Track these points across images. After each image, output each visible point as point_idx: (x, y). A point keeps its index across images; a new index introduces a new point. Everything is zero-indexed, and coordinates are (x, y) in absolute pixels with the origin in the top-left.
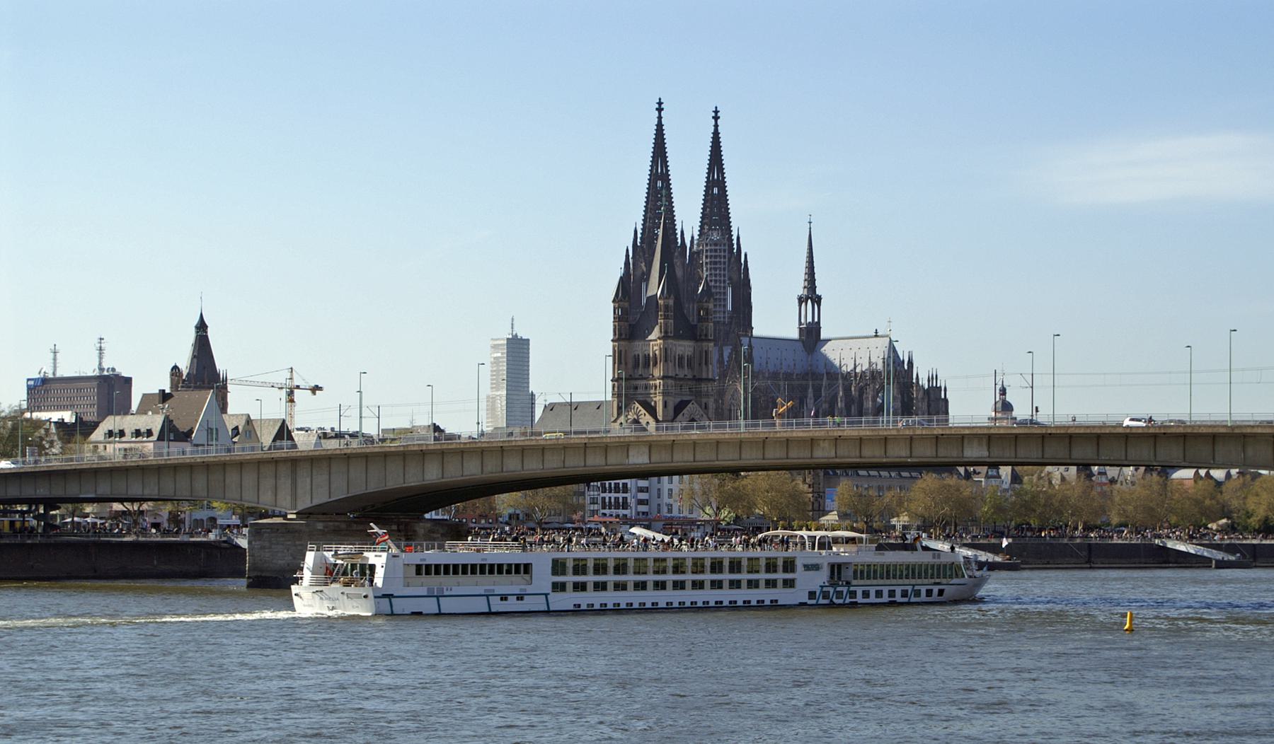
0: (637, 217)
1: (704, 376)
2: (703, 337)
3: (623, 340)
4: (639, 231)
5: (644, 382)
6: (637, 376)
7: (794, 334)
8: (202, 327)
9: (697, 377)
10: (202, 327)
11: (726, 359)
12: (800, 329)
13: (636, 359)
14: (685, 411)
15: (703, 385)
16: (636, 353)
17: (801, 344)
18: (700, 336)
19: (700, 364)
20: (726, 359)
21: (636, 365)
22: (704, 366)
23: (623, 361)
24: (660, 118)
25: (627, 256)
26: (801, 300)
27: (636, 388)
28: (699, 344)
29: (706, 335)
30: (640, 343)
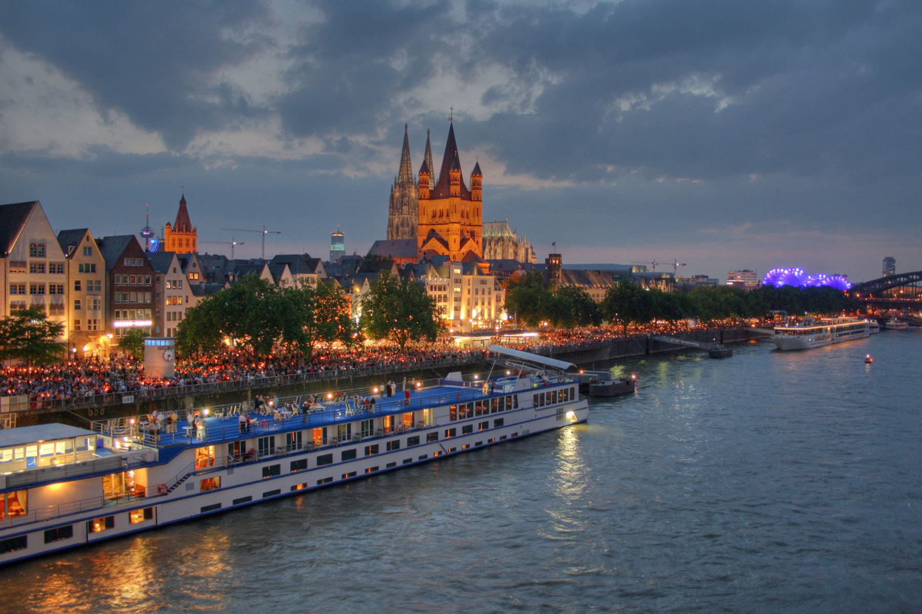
1: (477, 224)
3: (427, 199)
6: (435, 223)
8: (183, 202)
10: (183, 202)
21: (434, 216)
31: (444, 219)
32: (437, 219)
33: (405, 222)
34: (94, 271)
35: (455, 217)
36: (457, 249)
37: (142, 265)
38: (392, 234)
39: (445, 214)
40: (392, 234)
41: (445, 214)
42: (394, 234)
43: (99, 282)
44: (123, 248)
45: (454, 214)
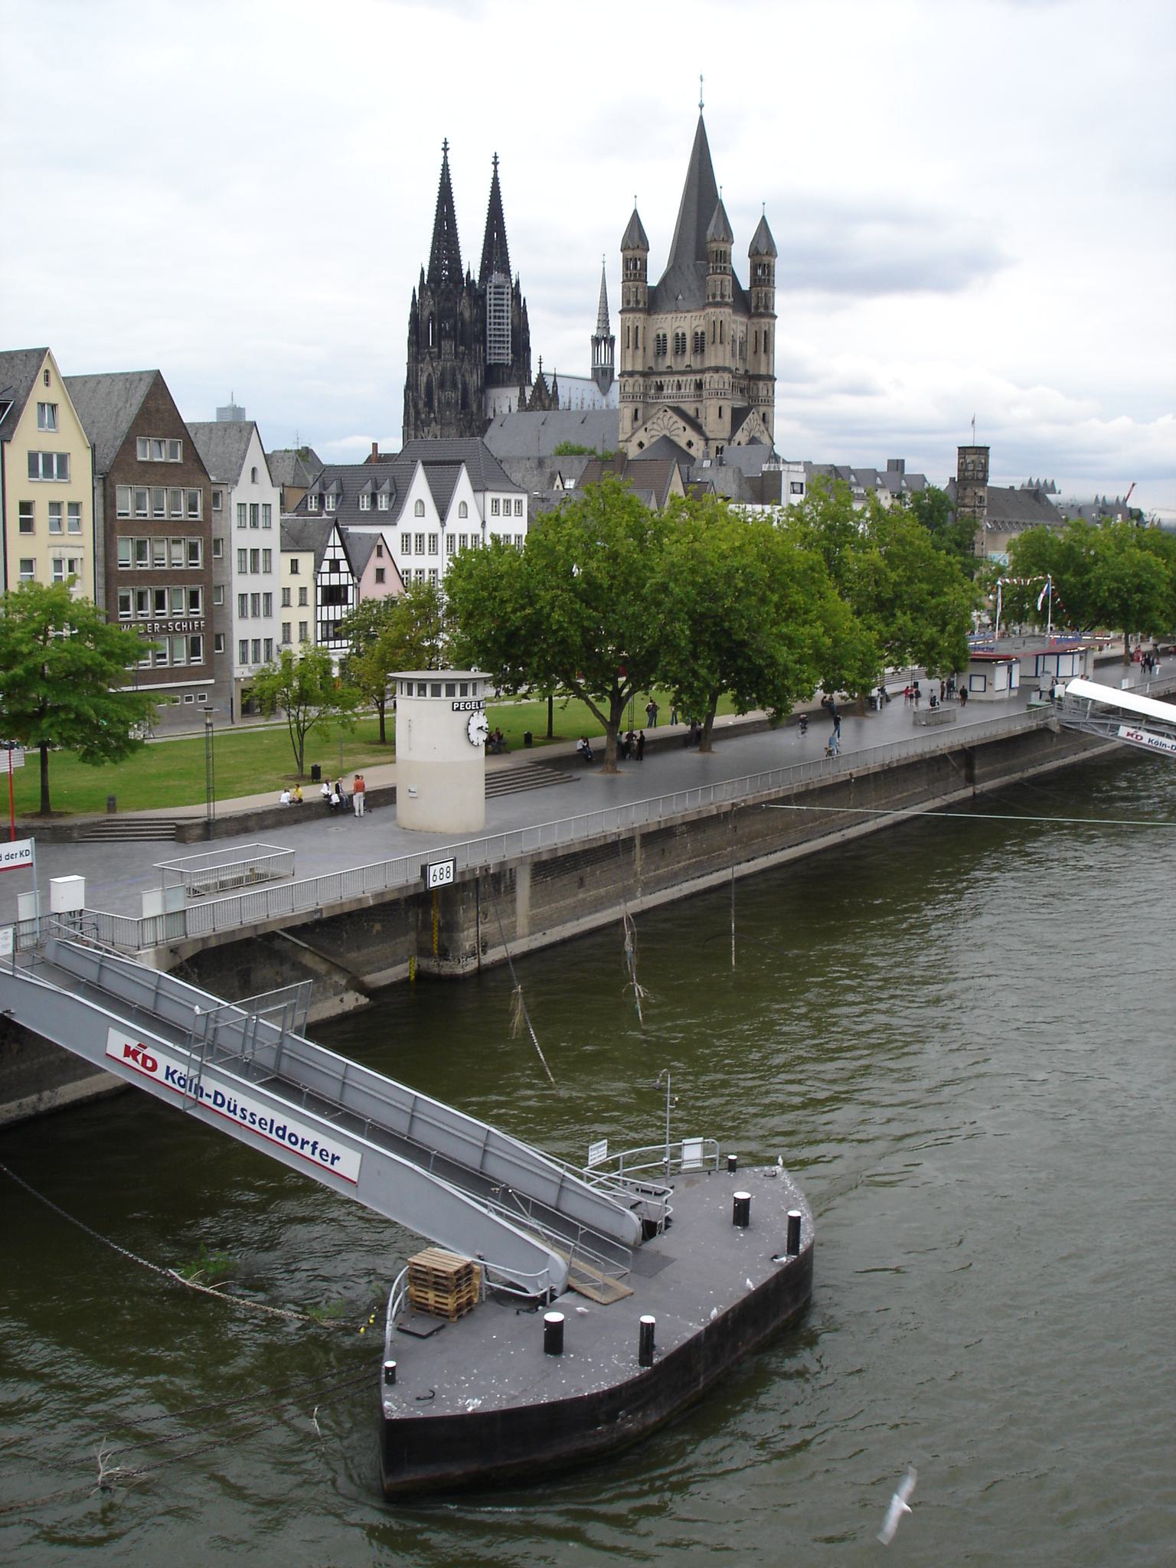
0: (422, 258)
2: (762, 310)
4: (426, 273)
5: (676, 378)
7: (589, 375)
9: (750, 373)
11: (528, 397)
12: (594, 370)
13: (661, 342)
14: (744, 425)
15: (761, 384)
16: (661, 332)
17: (594, 385)
18: (757, 307)
19: (755, 352)
20: (528, 397)
21: (661, 350)
22: (763, 356)
23: (640, 345)
24: (446, 158)
25: (414, 296)
26: (596, 341)
27: (660, 388)
28: (755, 320)
29: (766, 307)
30: (669, 316)
31: (689, 359)
32: (669, 360)
33: (448, 377)
34: (63, 472)
35: (720, 354)
36: (726, 434)
37: (179, 460)
38: (416, 406)
39: (689, 344)
40: (416, 406)
41: (689, 344)
42: (421, 405)
43: (75, 507)
44: (133, 409)
45: (720, 347)
